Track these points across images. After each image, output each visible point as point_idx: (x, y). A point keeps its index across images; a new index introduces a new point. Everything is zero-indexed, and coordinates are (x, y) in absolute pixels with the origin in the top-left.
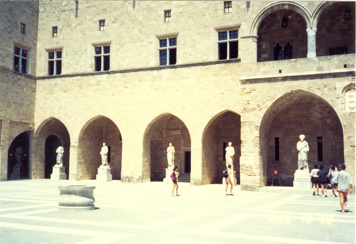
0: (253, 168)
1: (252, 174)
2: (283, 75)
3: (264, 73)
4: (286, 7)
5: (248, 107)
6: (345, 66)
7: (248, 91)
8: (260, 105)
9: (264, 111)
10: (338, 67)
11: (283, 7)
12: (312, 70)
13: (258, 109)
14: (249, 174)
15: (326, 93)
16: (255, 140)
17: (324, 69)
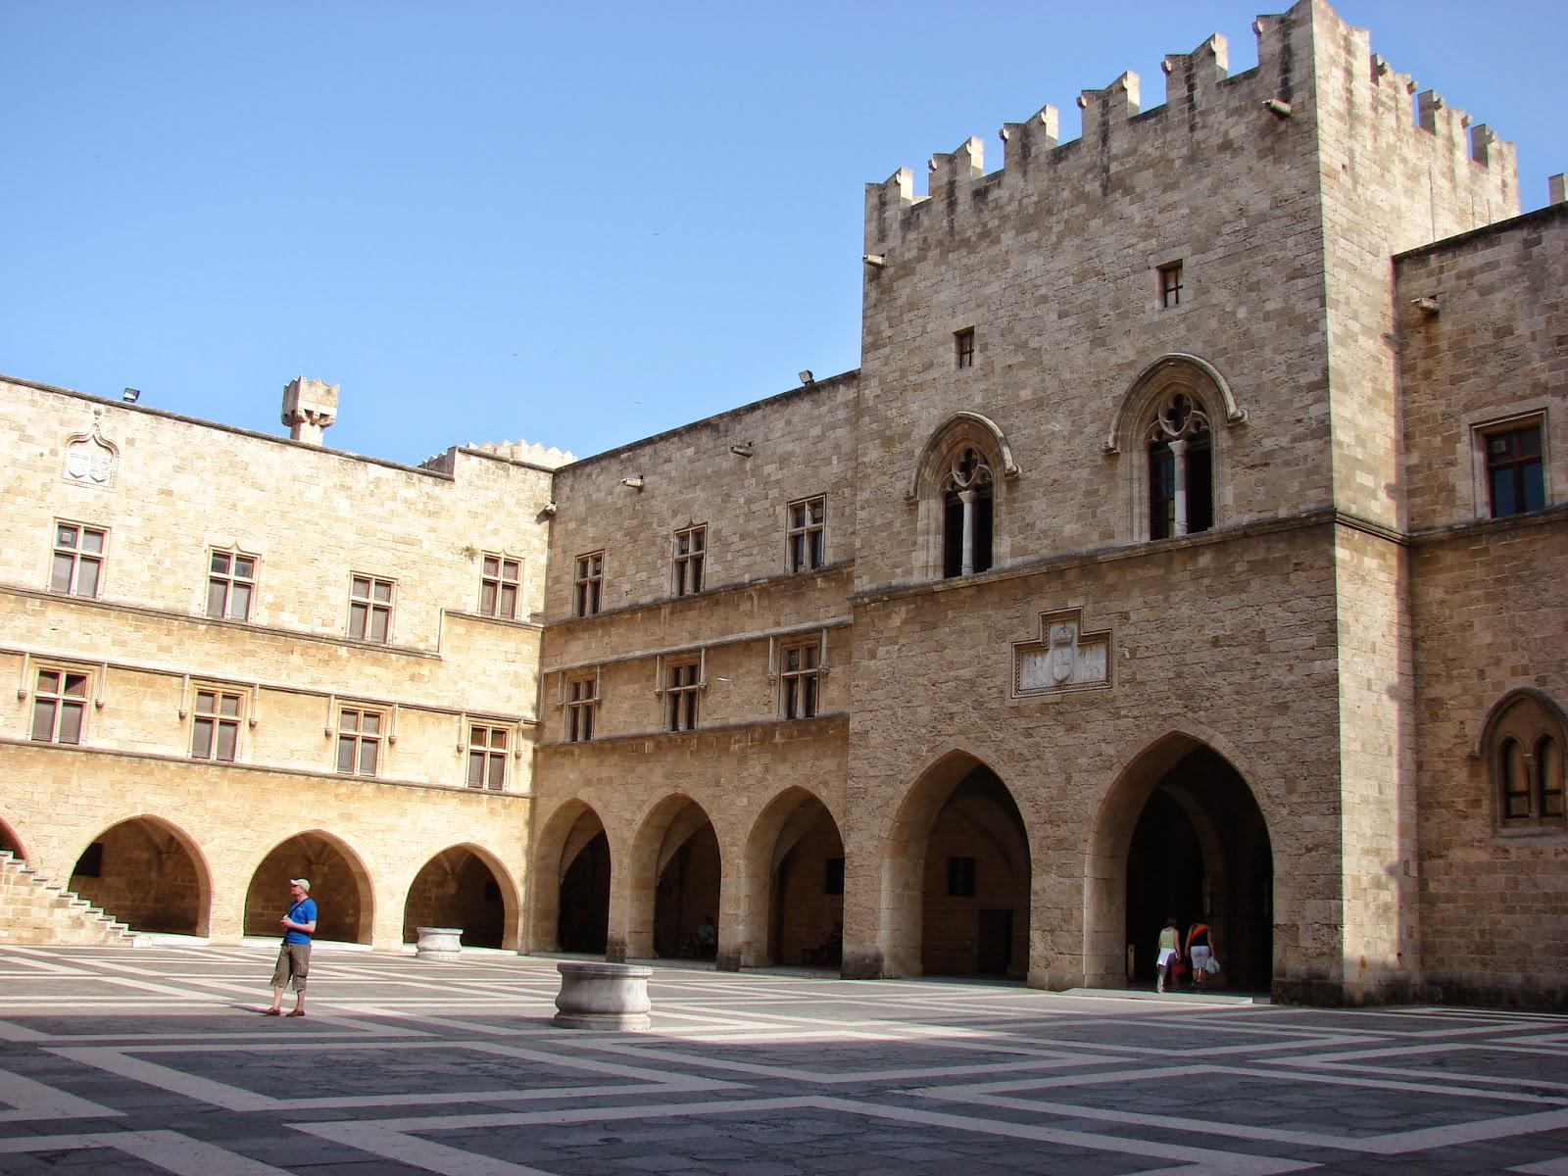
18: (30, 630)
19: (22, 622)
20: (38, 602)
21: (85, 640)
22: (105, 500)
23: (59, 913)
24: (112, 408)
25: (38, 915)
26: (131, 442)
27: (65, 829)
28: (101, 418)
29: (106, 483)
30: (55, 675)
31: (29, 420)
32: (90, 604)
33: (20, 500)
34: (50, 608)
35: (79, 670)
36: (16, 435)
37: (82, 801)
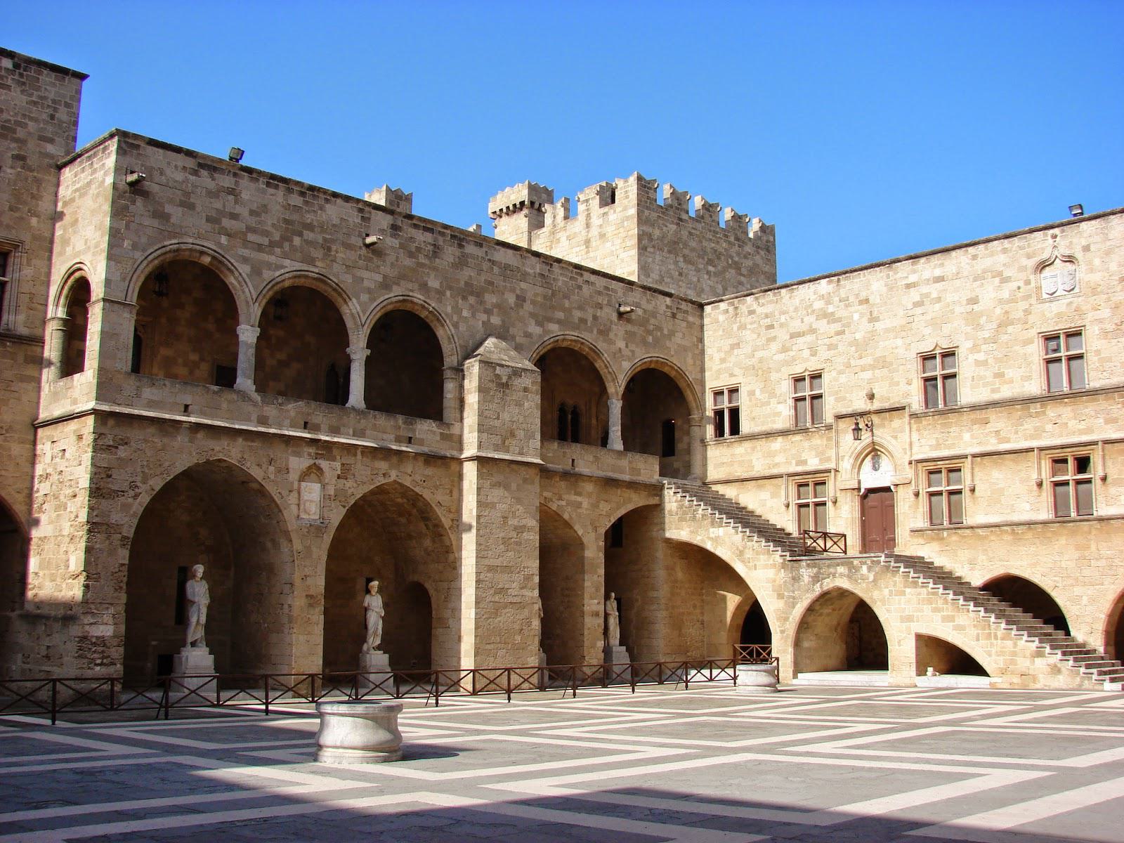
0: (108, 645)
1: (105, 661)
2: (193, 419)
3: (151, 405)
4: (206, 260)
5: (110, 486)
6: (306, 426)
7: (111, 443)
8: (139, 484)
9: (145, 499)
10: (293, 426)
11: (200, 256)
12: (248, 420)
13: (132, 493)
14: (99, 661)
15: (272, 477)
16: (120, 574)
17: (270, 422)
18: (1036, 429)
19: (1029, 425)
20: (1038, 405)
21: (1082, 426)
22: (1075, 305)
23: (1038, 661)
24: (1065, 228)
25: (1023, 664)
26: (1086, 249)
27: (1092, 588)
28: (1058, 239)
29: (1075, 291)
30: (1065, 461)
31: (1004, 265)
32: (1078, 395)
33: (1010, 329)
34: (1049, 407)
35: (1082, 452)
36: (997, 280)
37: (1102, 563)
